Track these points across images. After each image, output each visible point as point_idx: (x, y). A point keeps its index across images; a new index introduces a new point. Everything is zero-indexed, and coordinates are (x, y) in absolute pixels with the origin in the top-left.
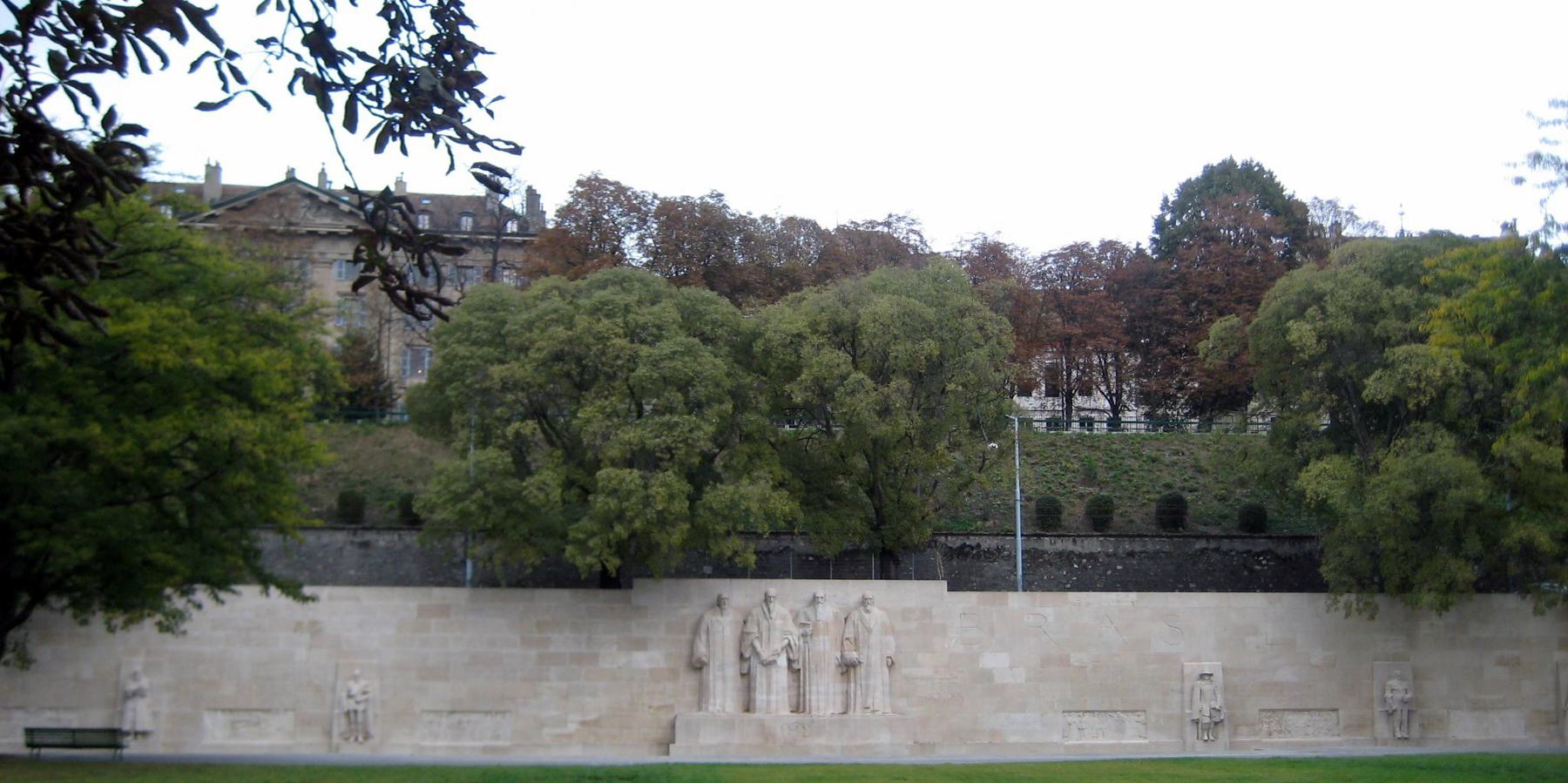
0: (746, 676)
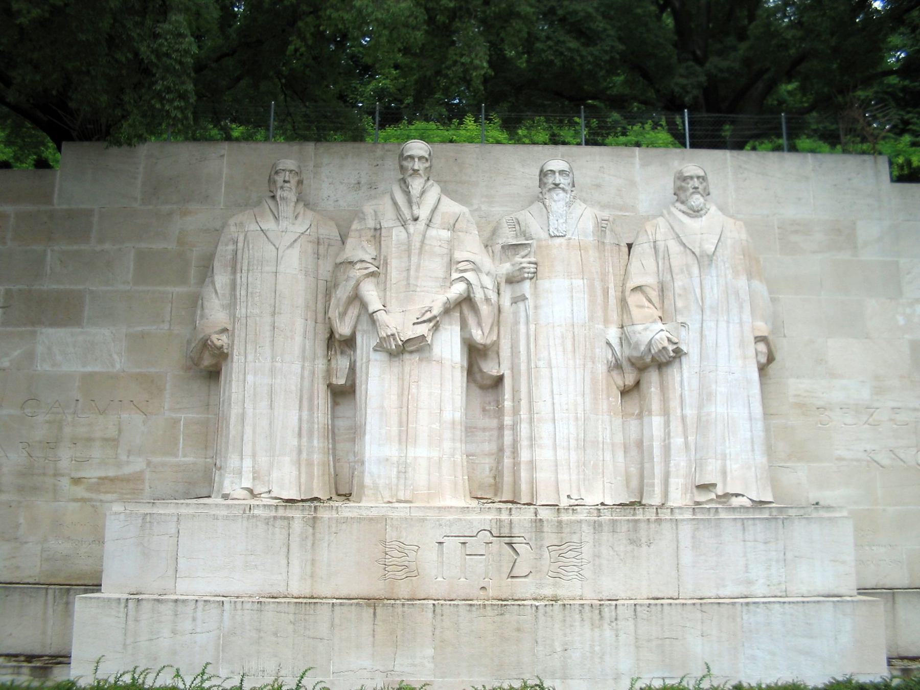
0: (343, 393)
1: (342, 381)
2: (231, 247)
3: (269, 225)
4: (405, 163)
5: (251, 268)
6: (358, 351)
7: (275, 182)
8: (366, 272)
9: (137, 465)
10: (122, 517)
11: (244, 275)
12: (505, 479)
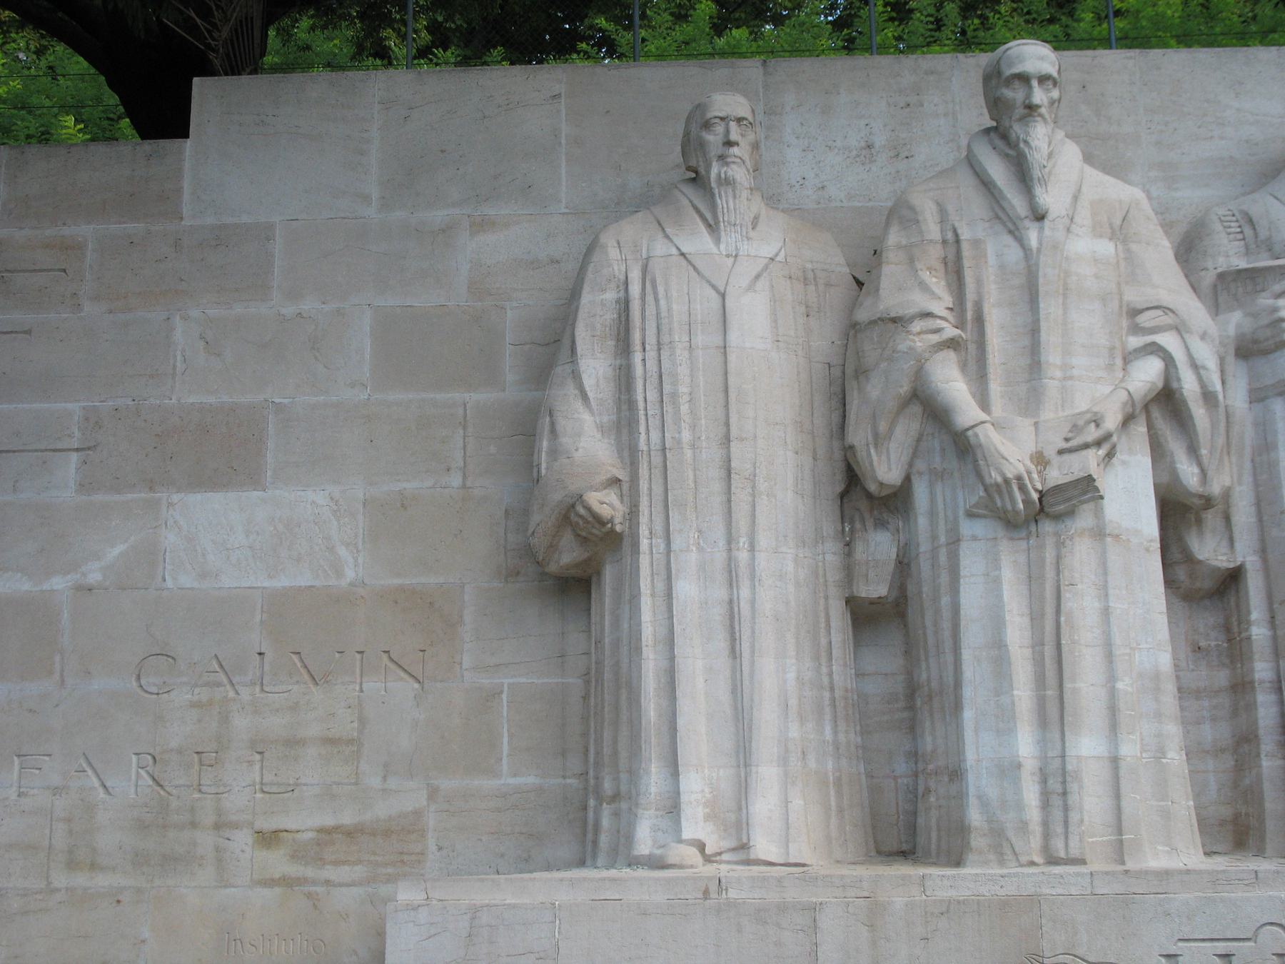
1: (876, 588)
2: (611, 295)
3: (697, 242)
4: (1008, 93)
5: (665, 339)
6: (922, 522)
7: (702, 145)
8: (935, 338)
9: (410, 797)
10: (423, 915)
11: (651, 354)
12: (1269, 806)
